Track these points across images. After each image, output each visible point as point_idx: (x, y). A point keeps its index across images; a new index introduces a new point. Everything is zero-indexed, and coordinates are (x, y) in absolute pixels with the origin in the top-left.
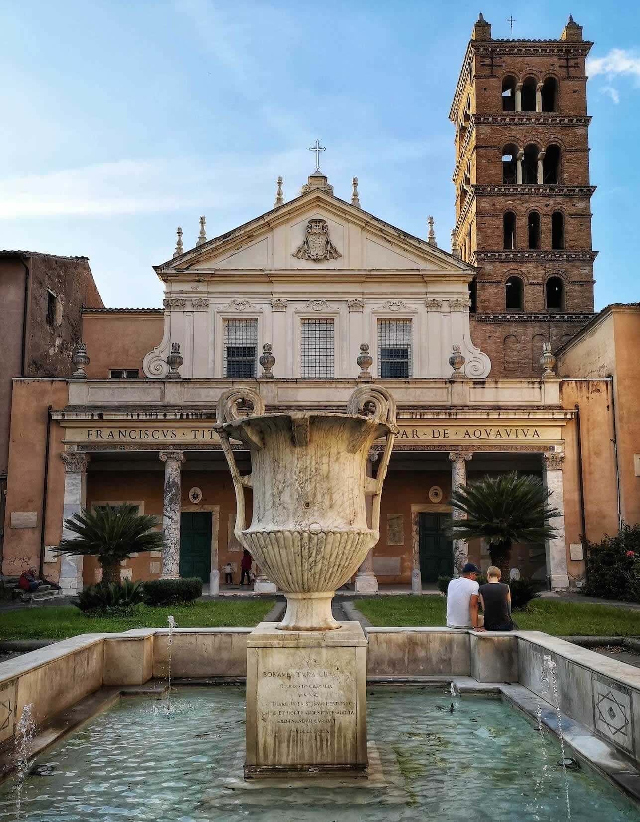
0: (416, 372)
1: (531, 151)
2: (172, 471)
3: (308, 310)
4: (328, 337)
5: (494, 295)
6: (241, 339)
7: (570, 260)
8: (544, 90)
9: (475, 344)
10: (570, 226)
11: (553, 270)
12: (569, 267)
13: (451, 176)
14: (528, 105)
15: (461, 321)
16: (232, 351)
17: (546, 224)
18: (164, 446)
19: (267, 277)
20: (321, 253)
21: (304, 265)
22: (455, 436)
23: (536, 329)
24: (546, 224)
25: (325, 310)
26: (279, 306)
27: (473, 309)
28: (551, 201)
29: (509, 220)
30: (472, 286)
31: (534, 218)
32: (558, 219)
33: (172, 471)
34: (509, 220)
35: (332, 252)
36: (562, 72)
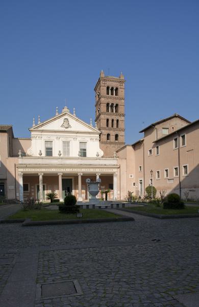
0: (88, 155)
1: (113, 104)
2: (41, 177)
3: (64, 140)
4: (68, 146)
5: (104, 137)
6: (49, 146)
7: (120, 131)
8: (115, 90)
9: (100, 148)
10: (120, 123)
11: (117, 132)
12: (119, 132)
13: (95, 104)
14: (112, 94)
15: (98, 143)
16: (47, 149)
17: (115, 122)
18: (39, 172)
19: (55, 132)
20: (67, 126)
21: (63, 129)
22: (97, 170)
23: (113, 145)
24: (115, 122)
25: (69, 139)
26: (58, 138)
27: (100, 141)
28: (116, 117)
29: (108, 120)
30: (100, 135)
31: (113, 120)
32: (118, 121)
33: (41, 177)
34: (108, 120)
35: (69, 126)
36: (119, 87)
